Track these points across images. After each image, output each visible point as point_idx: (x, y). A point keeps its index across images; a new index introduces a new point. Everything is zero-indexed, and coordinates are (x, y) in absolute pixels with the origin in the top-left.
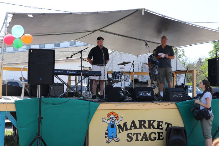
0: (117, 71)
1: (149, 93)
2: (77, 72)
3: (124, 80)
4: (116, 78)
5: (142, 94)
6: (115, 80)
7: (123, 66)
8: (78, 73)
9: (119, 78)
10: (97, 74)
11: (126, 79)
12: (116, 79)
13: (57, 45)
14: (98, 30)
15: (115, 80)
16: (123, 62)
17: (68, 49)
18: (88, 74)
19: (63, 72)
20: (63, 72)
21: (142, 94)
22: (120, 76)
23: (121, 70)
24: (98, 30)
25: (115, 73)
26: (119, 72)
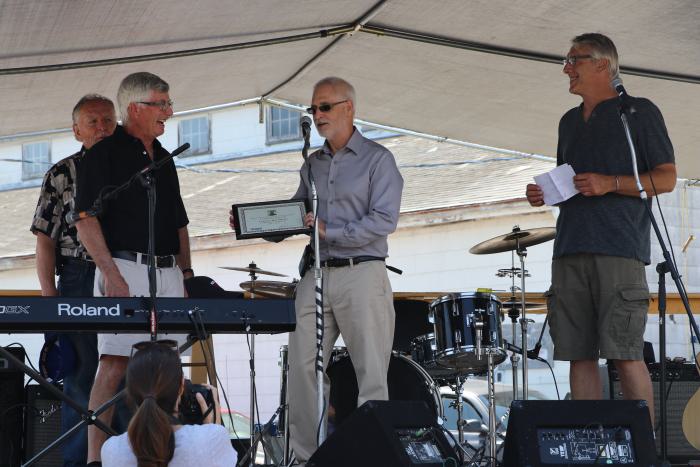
0: (468, 290)
1: (619, 440)
2: (125, 312)
3: (521, 352)
4: (458, 339)
5: (562, 450)
6: (450, 352)
7: (507, 259)
8: (131, 312)
9: (475, 344)
10: (260, 321)
11: (538, 347)
12: (454, 345)
13: (285, 132)
14: (353, 25)
15: (450, 352)
16: (509, 231)
17: (265, 163)
18: (202, 321)
19: (24, 310)
20: (24, 310)
21: (562, 450)
22: (486, 331)
23: (504, 285)
24: (353, 25)
25: (450, 303)
26: (481, 300)
